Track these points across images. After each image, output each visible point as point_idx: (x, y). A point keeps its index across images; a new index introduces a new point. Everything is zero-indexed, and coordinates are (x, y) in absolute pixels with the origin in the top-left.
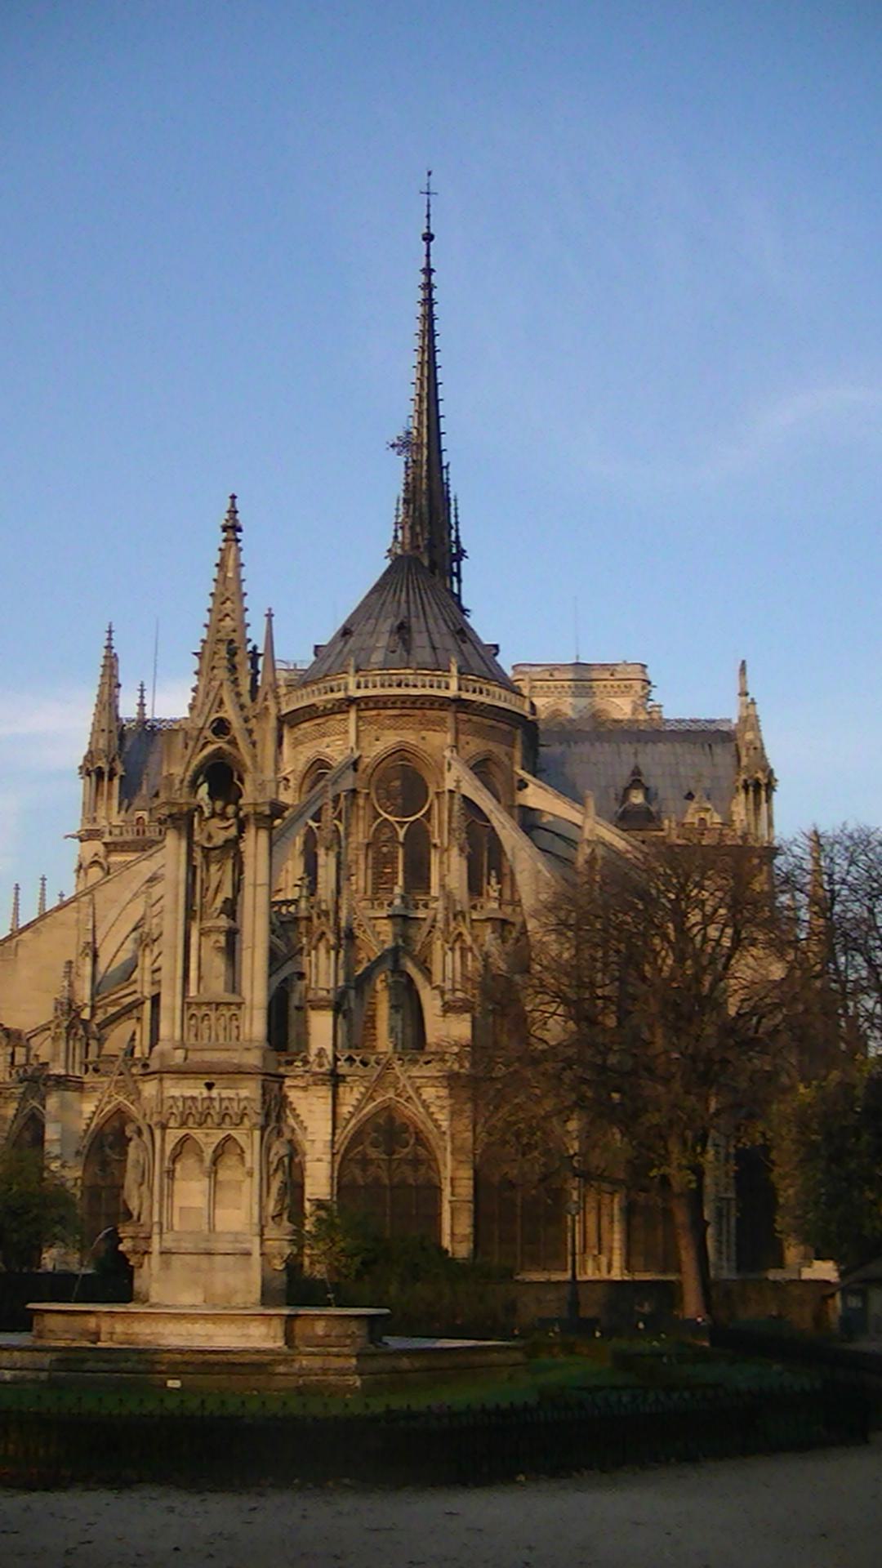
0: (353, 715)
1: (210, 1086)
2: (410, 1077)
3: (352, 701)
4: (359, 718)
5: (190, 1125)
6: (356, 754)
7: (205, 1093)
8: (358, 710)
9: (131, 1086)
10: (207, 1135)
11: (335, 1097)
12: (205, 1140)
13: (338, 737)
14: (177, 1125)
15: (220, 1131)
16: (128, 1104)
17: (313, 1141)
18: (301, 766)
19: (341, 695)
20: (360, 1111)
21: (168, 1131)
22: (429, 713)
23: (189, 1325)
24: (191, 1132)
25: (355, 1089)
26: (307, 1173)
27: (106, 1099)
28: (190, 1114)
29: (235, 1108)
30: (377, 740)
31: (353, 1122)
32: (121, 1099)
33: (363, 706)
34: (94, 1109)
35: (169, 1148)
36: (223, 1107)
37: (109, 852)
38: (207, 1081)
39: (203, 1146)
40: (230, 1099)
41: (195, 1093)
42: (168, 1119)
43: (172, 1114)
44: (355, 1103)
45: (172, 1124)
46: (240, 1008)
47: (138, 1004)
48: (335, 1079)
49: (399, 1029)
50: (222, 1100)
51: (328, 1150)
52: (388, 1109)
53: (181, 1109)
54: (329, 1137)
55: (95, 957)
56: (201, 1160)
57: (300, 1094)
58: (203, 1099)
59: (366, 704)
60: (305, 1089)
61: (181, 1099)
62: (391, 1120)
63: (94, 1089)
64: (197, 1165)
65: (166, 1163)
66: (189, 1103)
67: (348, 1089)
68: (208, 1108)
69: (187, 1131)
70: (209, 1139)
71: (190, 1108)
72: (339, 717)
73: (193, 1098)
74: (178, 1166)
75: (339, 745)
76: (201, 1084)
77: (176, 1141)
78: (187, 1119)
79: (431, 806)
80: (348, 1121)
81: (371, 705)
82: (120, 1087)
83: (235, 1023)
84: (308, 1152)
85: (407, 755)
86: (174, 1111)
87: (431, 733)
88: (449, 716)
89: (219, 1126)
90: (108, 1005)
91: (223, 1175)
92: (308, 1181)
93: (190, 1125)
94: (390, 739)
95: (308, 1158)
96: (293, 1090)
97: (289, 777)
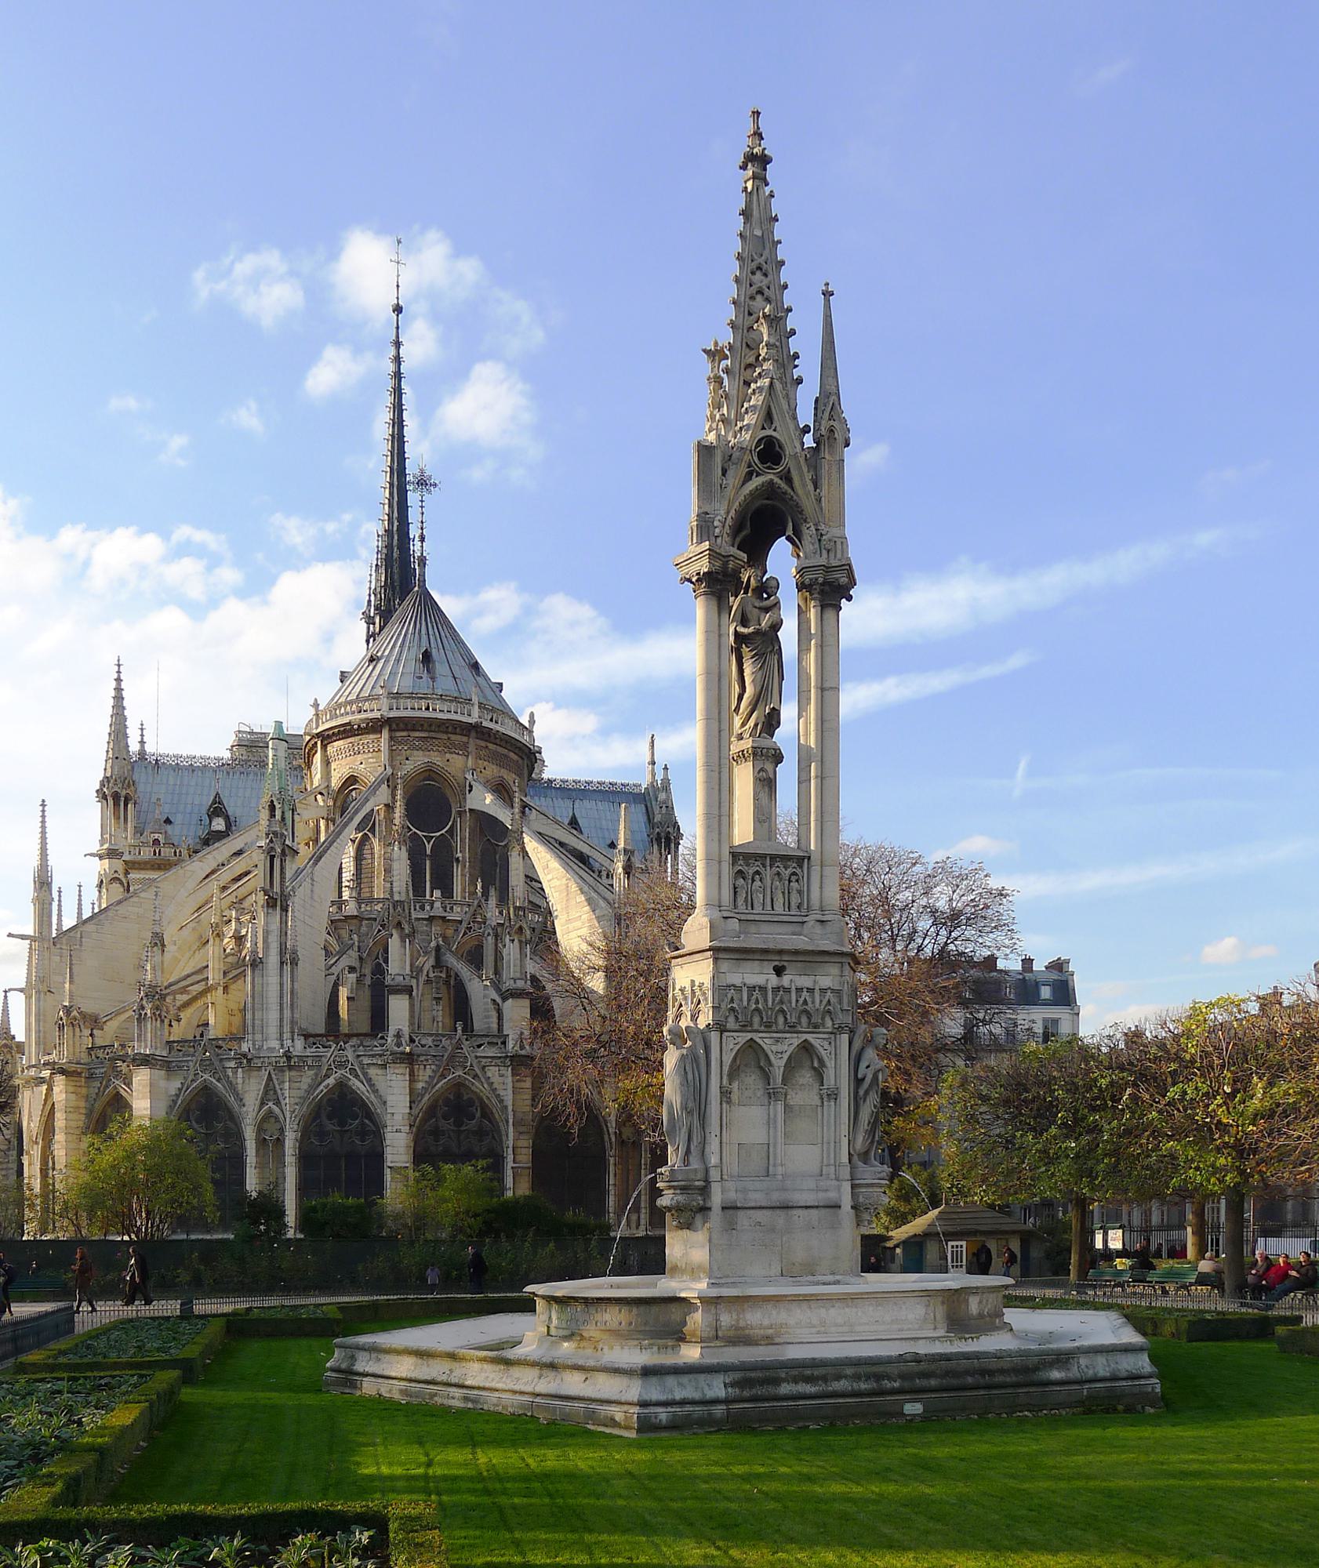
0: (385, 733)
1: (779, 971)
2: (477, 1057)
3: (387, 722)
4: (391, 738)
5: (756, 1026)
6: (389, 771)
7: (773, 980)
8: (390, 730)
9: (217, 1063)
10: (777, 1040)
11: (412, 1074)
12: (774, 1048)
13: (370, 755)
14: (737, 1028)
15: (796, 1035)
16: (214, 1081)
17: (393, 1114)
18: (336, 782)
19: (376, 715)
20: (433, 1088)
21: (726, 1034)
22: (453, 737)
23: (823, 1311)
24: (756, 1037)
25: (428, 1067)
26: (388, 1142)
27: (190, 1079)
28: (757, 1009)
29: (817, 1003)
30: (407, 759)
31: (426, 1098)
32: (206, 1076)
33: (394, 726)
34: (180, 1086)
35: (728, 1059)
36: (801, 1000)
37: (127, 873)
38: (776, 963)
39: (772, 1058)
40: (810, 990)
41: (759, 980)
42: (727, 1017)
43: (732, 1009)
44: (427, 1078)
45: (731, 1024)
46: (801, 867)
47: (214, 988)
48: (410, 1059)
49: (440, 1019)
50: (799, 990)
51: (407, 1122)
52: (459, 1086)
53: (745, 1003)
54: (408, 1111)
55: (163, 945)
56: (766, 1077)
57: (380, 1072)
58: (776, 989)
59: (397, 725)
60: (384, 1066)
61: (745, 990)
62: (459, 1096)
63: (180, 1068)
64: (760, 1084)
65: (725, 1081)
66: (756, 994)
67: (422, 1067)
68: (781, 1002)
69: (749, 1036)
70: (779, 1049)
71: (757, 1002)
72: (372, 736)
73: (763, 989)
74: (735, 1085)
75: (371, 763)
76: (769, 968)
77: (738, 1047)
78: (751, 1017)
79: (453, 824)
80: (423, 1096)
81: (401, 725)
82: (206, 1064)
83: (794, 885)
84: (388, 1123)
85: (434, 775)
86: (734, 1005)
87: (454, 755)
88: (473, 742)
89: (792, 1028)
90: (174, 993)
91: (797, 1098)
92: (388, 1151)
93: (756, 1026)
94: (416, 761)
95: (389, 1129)
96: (372, 1067)
97: (323, 792)
